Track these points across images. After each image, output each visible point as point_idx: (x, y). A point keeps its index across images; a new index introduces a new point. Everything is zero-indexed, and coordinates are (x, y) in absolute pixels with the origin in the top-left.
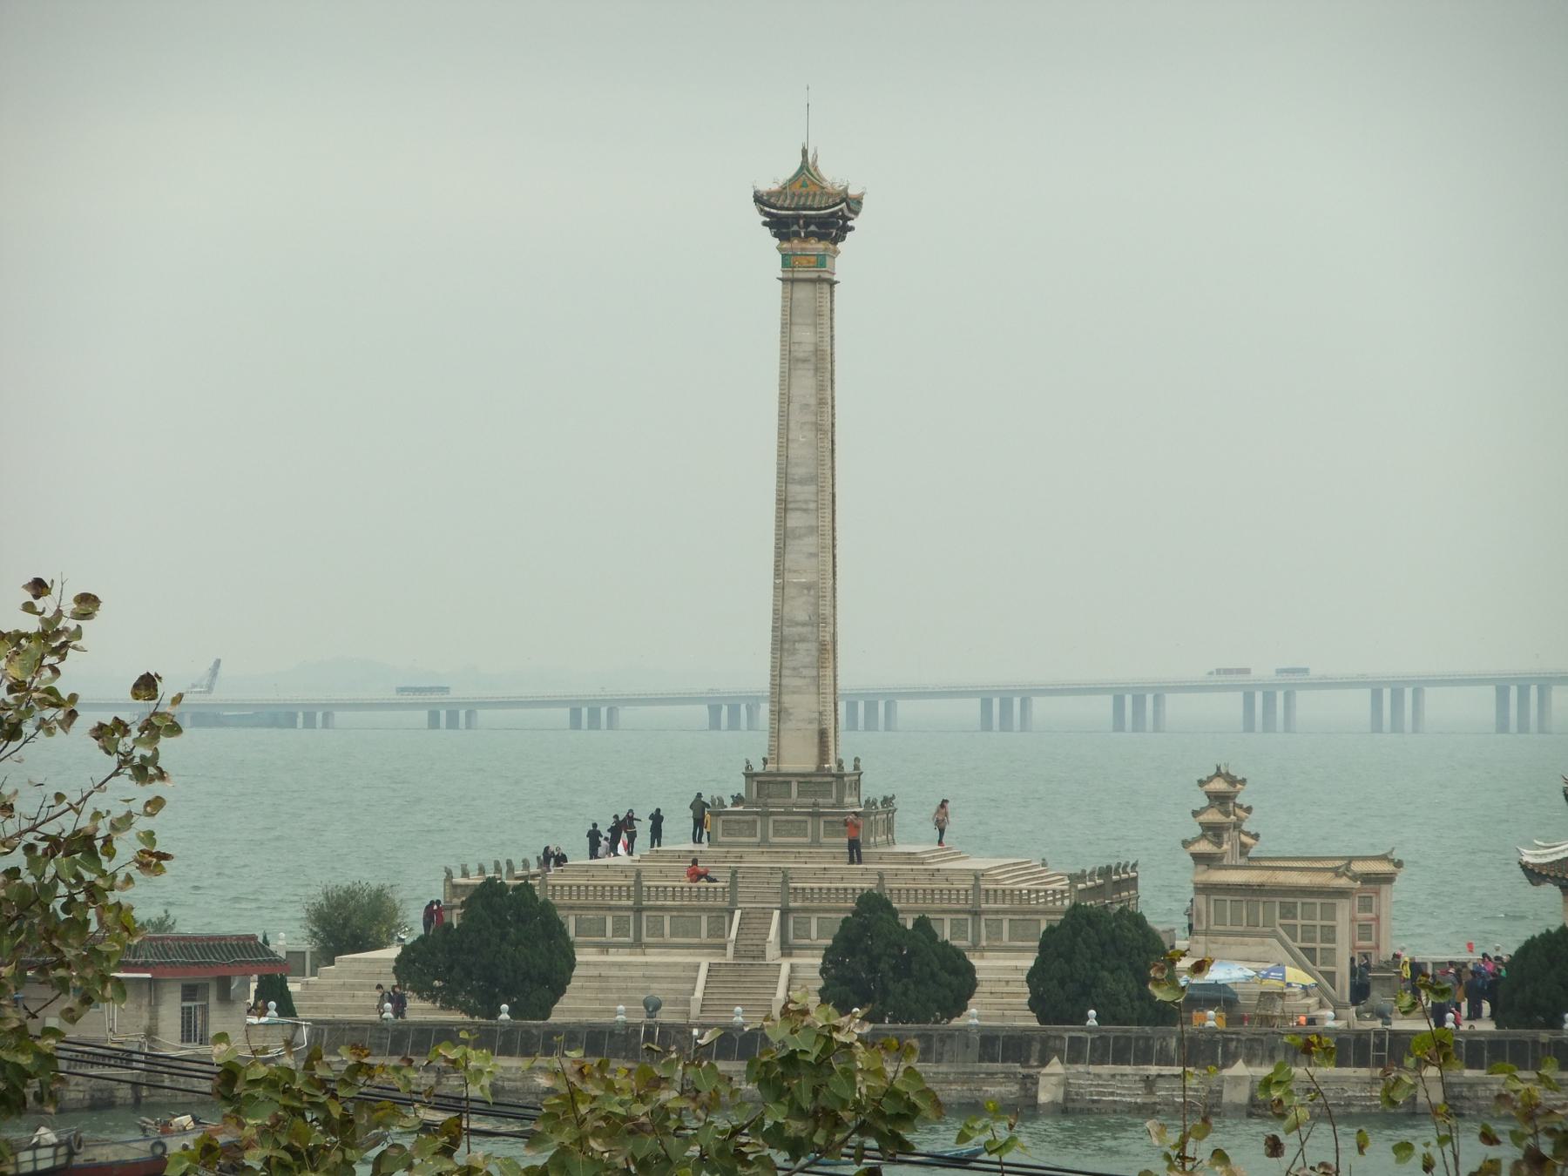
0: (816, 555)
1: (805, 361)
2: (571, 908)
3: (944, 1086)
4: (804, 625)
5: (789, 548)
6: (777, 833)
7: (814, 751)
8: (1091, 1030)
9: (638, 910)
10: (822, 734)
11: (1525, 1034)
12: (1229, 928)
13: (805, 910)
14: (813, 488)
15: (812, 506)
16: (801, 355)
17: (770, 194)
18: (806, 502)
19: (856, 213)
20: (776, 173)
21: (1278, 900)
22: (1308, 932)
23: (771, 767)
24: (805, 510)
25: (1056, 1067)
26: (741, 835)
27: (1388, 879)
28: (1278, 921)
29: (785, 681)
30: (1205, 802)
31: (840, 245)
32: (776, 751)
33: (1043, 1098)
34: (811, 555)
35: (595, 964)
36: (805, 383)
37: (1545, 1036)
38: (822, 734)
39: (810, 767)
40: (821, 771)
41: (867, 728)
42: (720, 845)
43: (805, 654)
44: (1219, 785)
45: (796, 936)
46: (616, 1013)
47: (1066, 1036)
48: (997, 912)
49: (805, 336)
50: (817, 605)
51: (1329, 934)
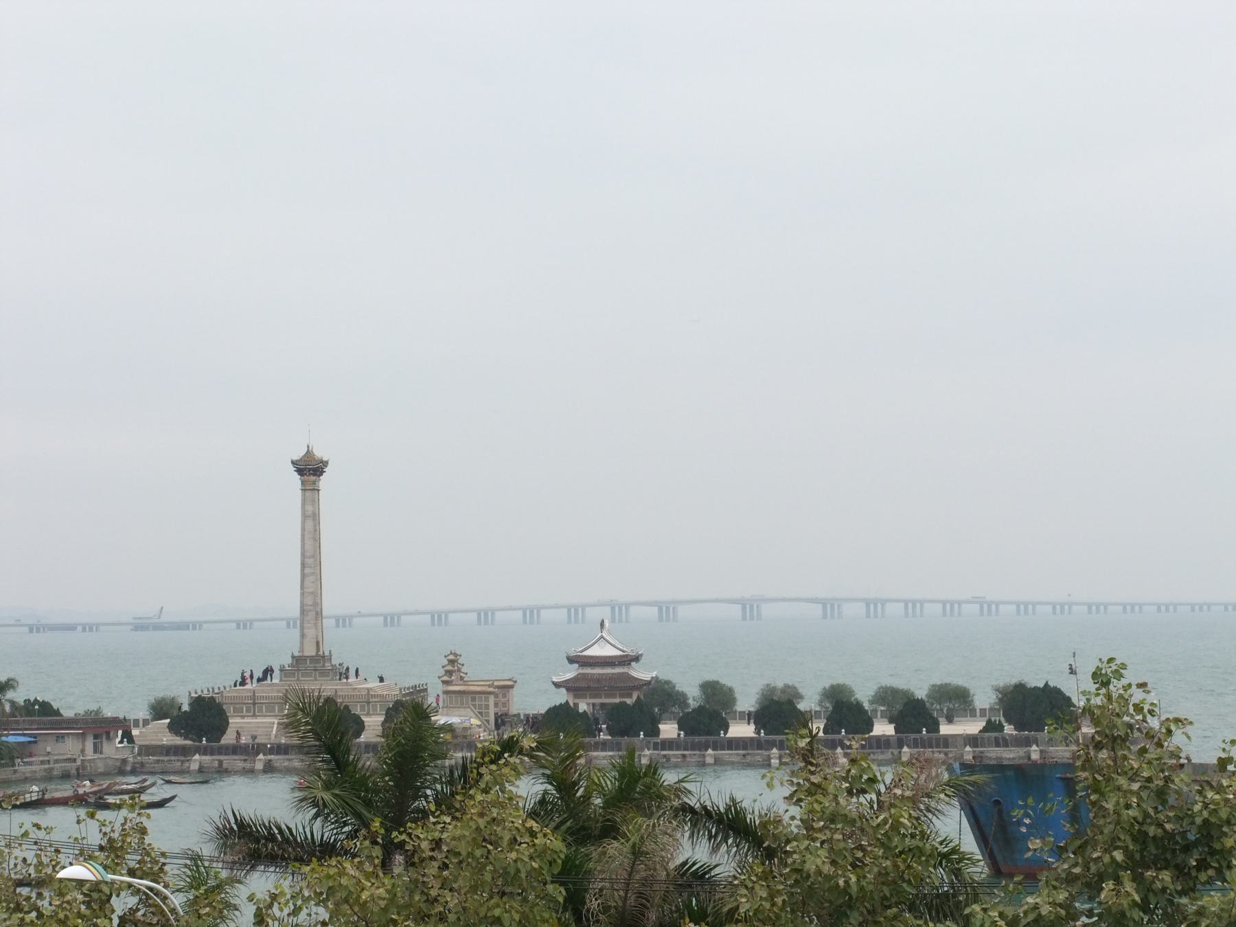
9: (254, 704)
10: (318, 643)
20: (299, 454)
22: (480, 706)
27: (512, 687)
32: (302, 650)
36: (310, 524)
38: (318, 643)
43: (311, 615)
44: (451, 657)
49: (309, 508)
51: (487, 707)
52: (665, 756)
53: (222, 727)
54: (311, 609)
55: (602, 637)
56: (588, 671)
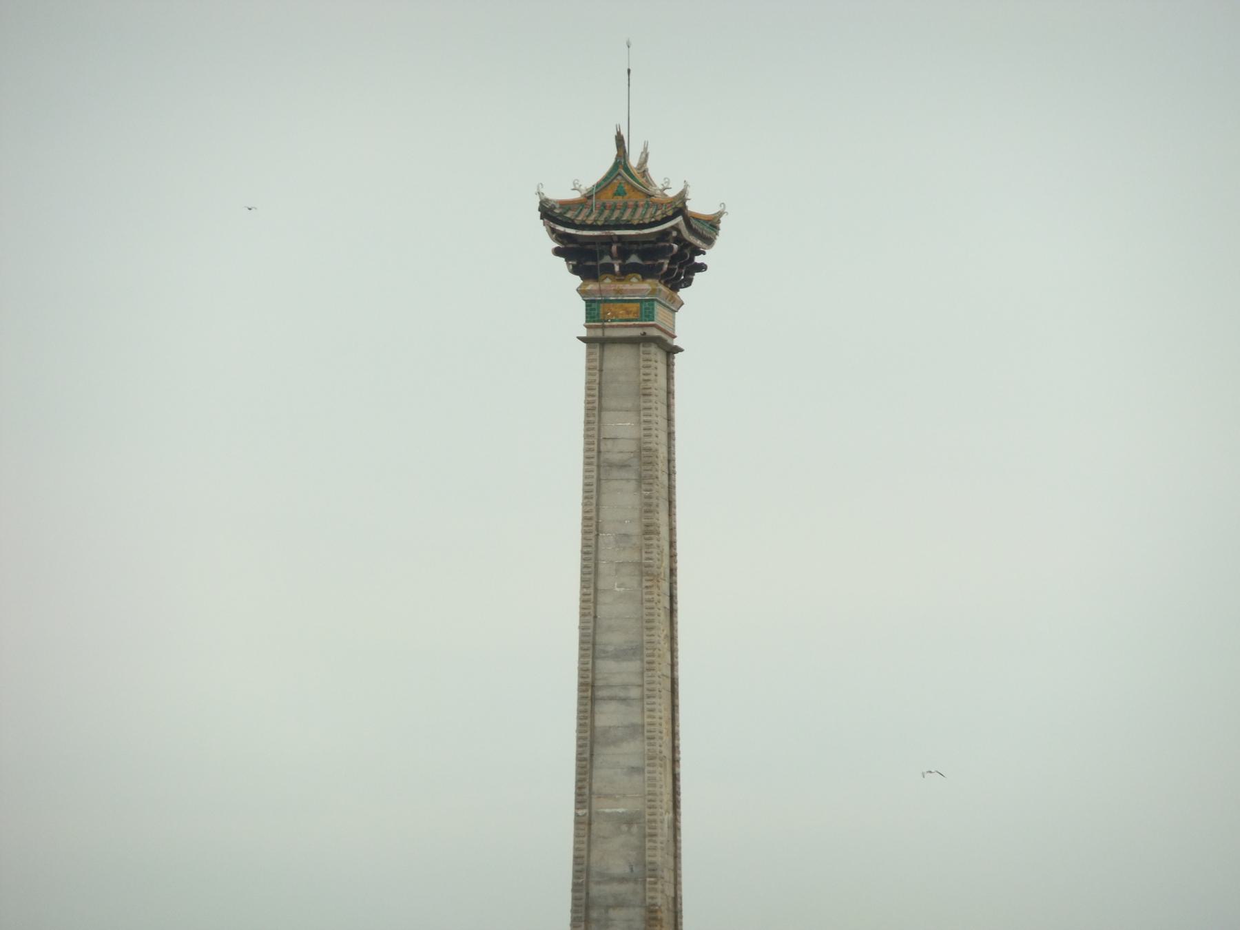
1: (623, 466)
16: (615, 457)
24: (624, 700)
36: (623, 501)
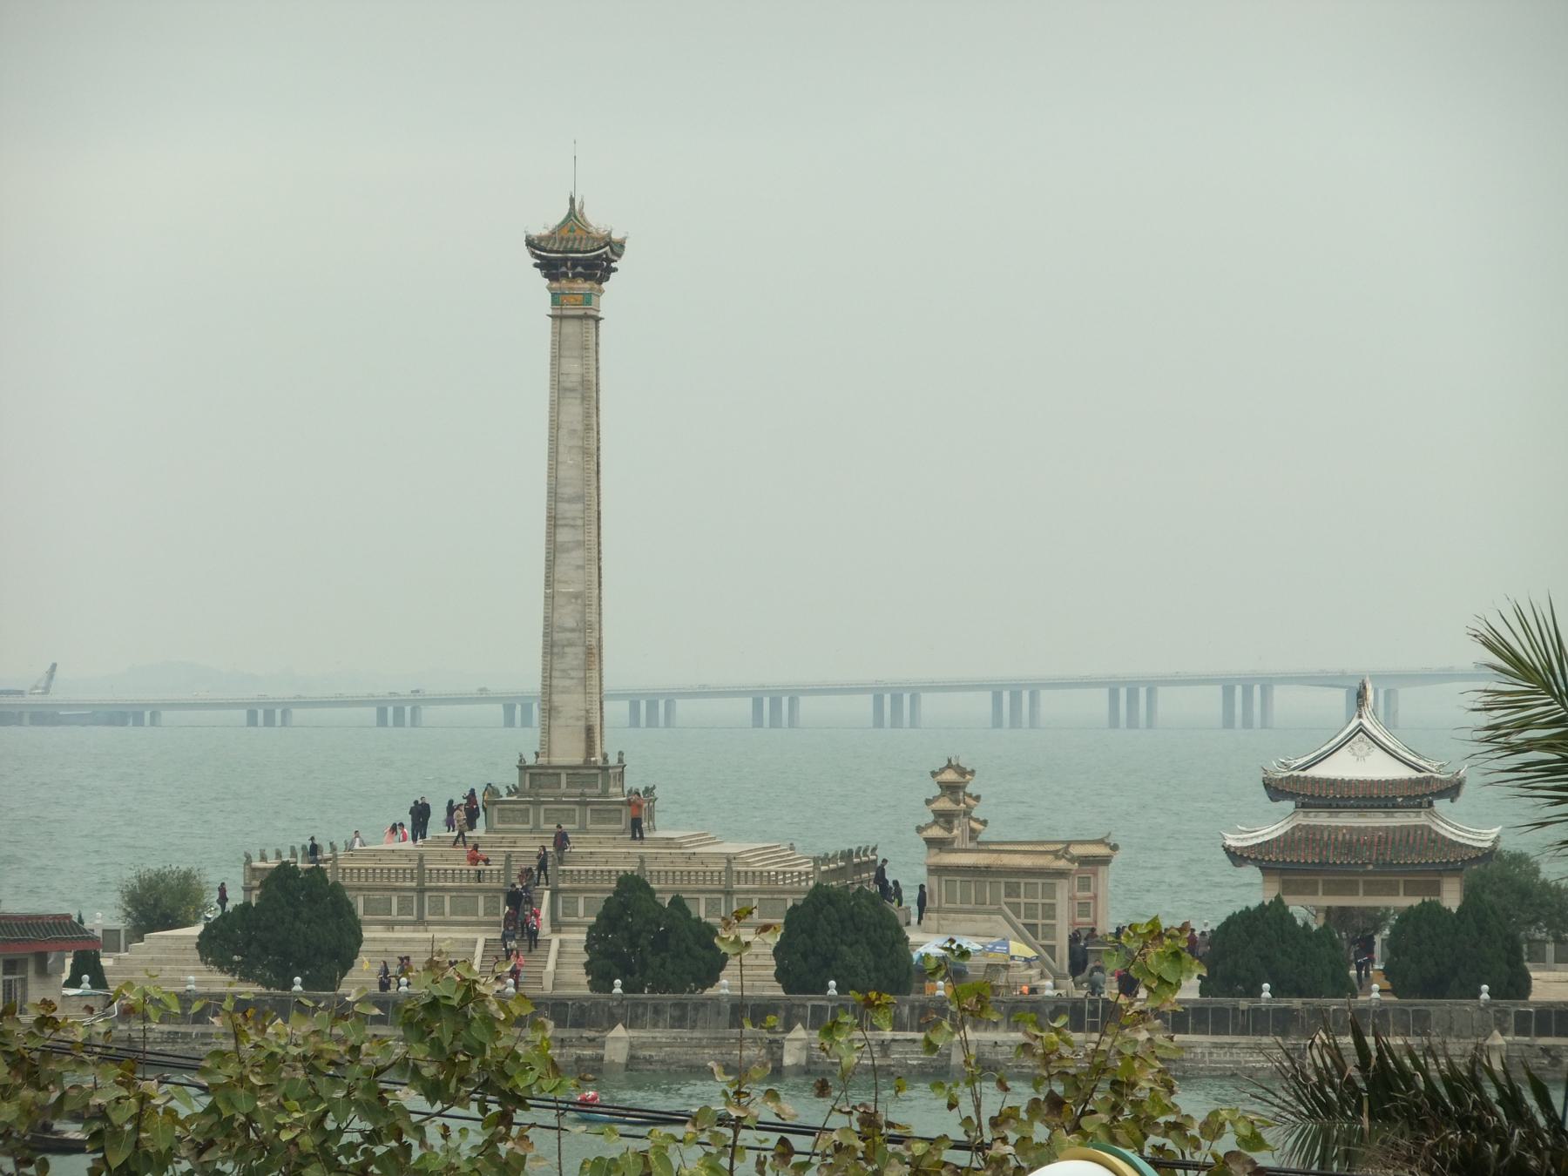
0: (583, 567)
1: (572, 390)
2: (360, 889)
3: (698, 1050)
4: (572, 630)
5: (558, 562)
6: (547, 820)
7: (582, 746)
8: (831, 999)
9: (421, 891)
10: (589, 730)
11: (1226, 1001)
12: (959, 906)
13: (574, 890)
14: (579, 506)
15: (580, 522)
16: (569, 385)
17: (541, 239)
18: (574, 519)
19: (619, 256)
20: (546, 220)
21: (1003, 880)
23: (542, 760)
25: (799, 1032)
26: (515, 822)
27: (1105, 861)
28: (1003, 899)
29: (555, 682)
30: (938, 791)
31: (604, 285)
32: (546, 746)
33: (788, 1060)
34: (578, 567)
35: (382, 940)
36: (573, 411)
37: (1244, 1004)
38: (589, 730)
39: (578, 760)
40: (588, 764)
41: (396, 724)
42: (496, 831)
43: (573, 657)
44: (950, 776)
45: (565, 914)
46: (187, 982)
47: (809, 1004)
48: (747, 892)
49: (572, 367)
50: (584, 613)
51: (1050, 911)
52: (1546, 1050)
53: (344, 953)
54: (573, 640)
55: (1361, 729)
56: (1322, 819)
